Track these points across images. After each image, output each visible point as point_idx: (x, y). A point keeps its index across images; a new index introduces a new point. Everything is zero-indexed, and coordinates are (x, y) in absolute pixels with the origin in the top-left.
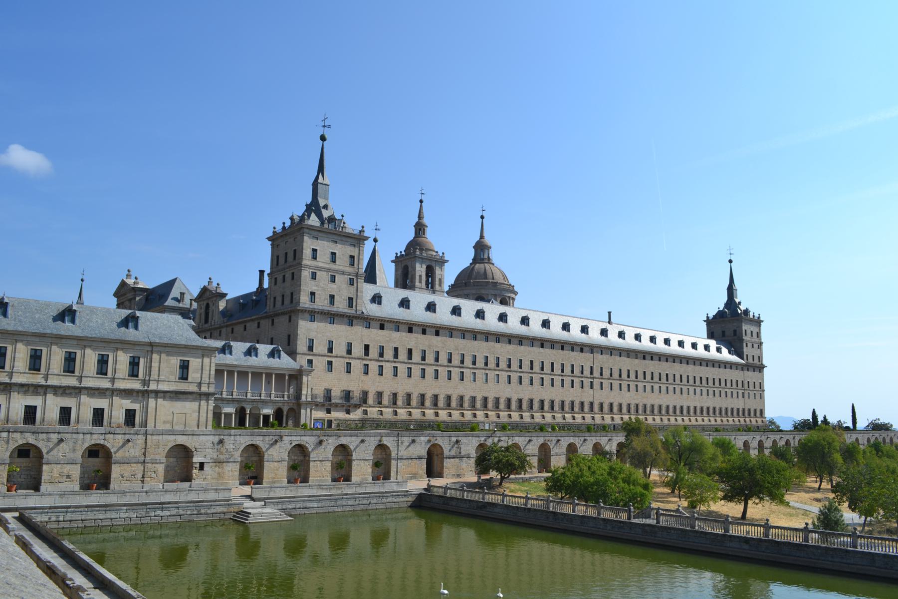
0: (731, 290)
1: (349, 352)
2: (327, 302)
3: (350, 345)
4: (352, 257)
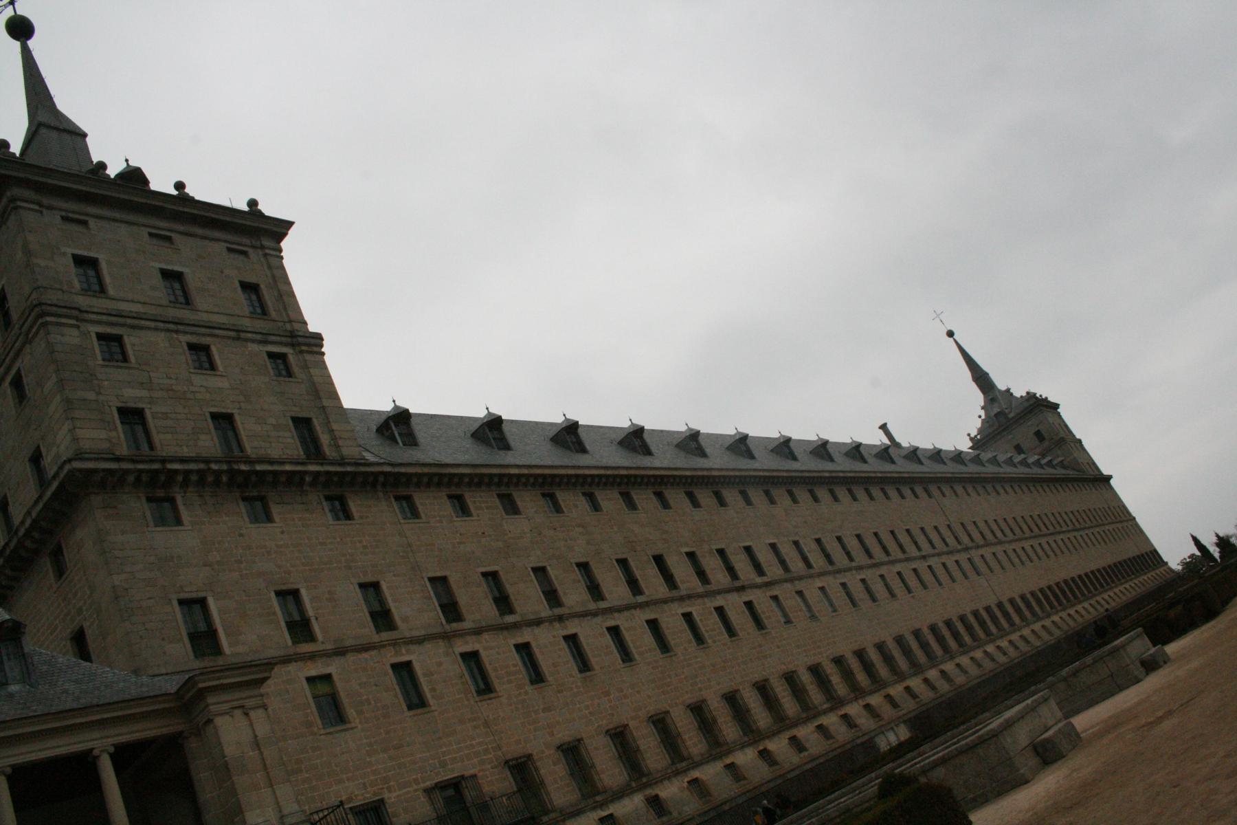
0: (982, 379)
1: (382, 618)
2: (209, 444)
3: (371, 588)
4: (250, 288)
